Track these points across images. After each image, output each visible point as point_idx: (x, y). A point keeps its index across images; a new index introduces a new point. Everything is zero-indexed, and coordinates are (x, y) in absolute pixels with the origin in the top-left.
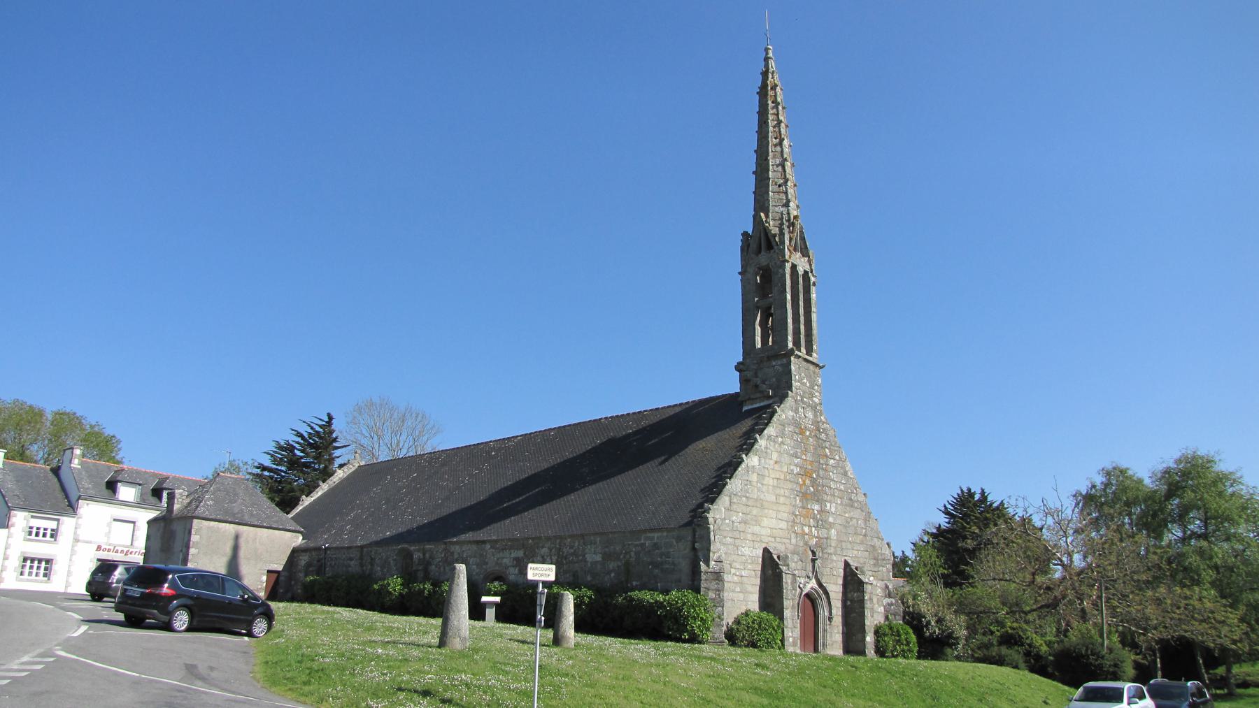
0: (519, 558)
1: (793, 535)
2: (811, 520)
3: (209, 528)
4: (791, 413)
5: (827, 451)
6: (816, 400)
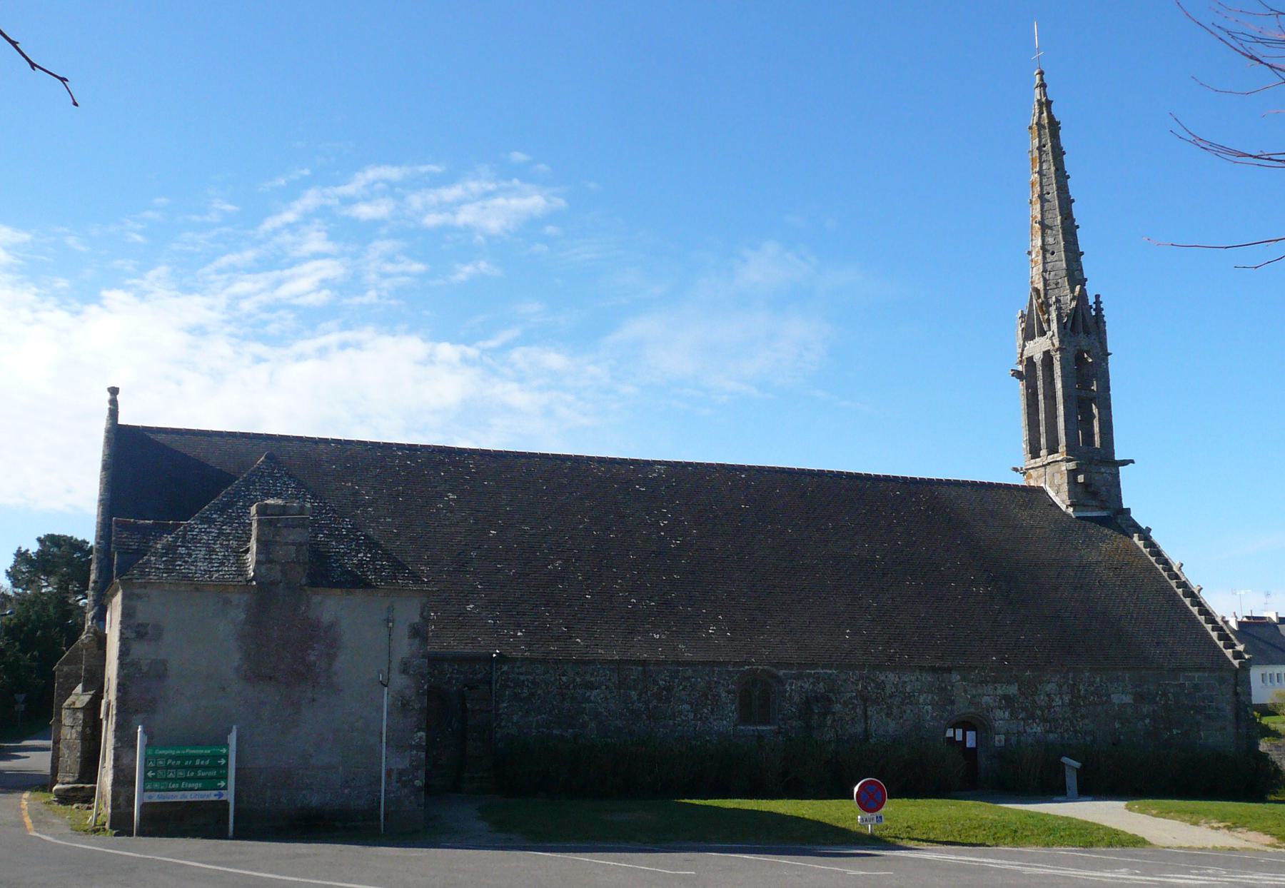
0: (1009, 696)
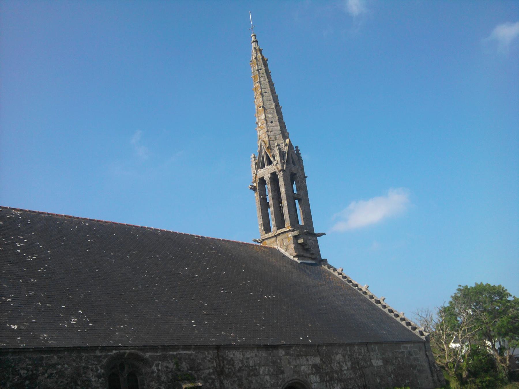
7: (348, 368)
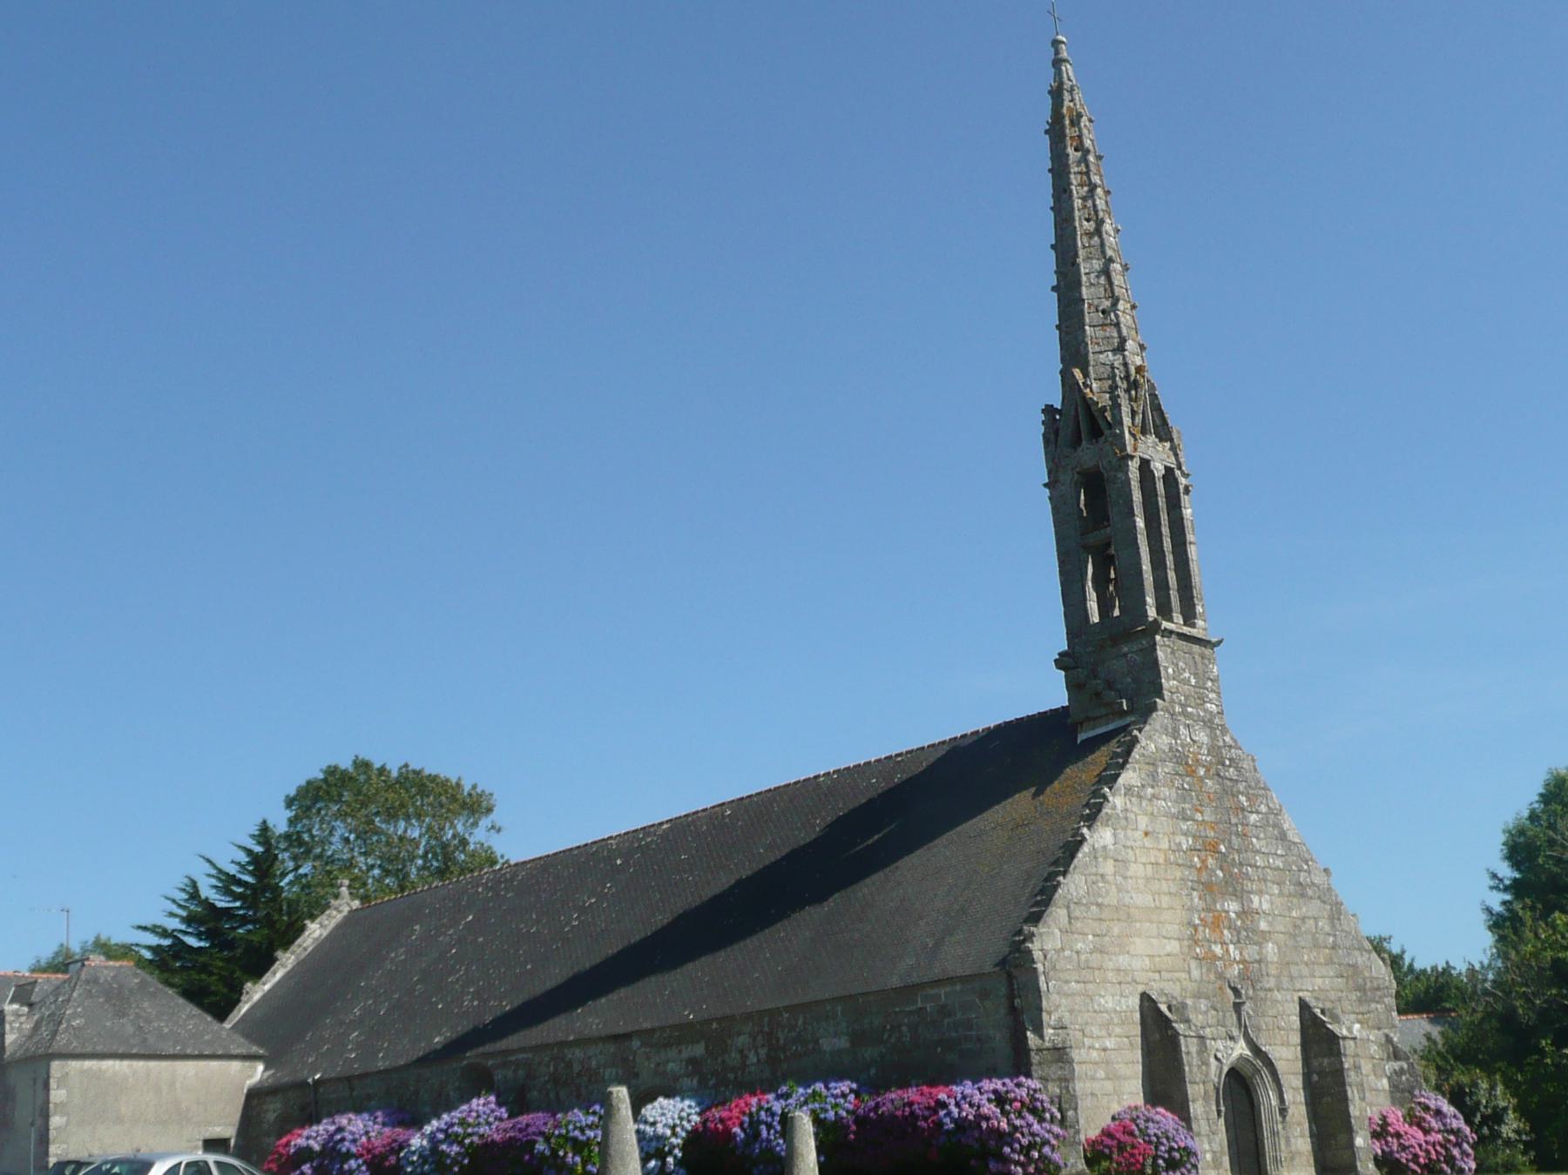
1: (1193, 964)
2: (1226, 932)
3: (82, 1072)
4: (1165, 740)
5: (1243, 799)
6: (1212, 707)
7: (758, 1060)
